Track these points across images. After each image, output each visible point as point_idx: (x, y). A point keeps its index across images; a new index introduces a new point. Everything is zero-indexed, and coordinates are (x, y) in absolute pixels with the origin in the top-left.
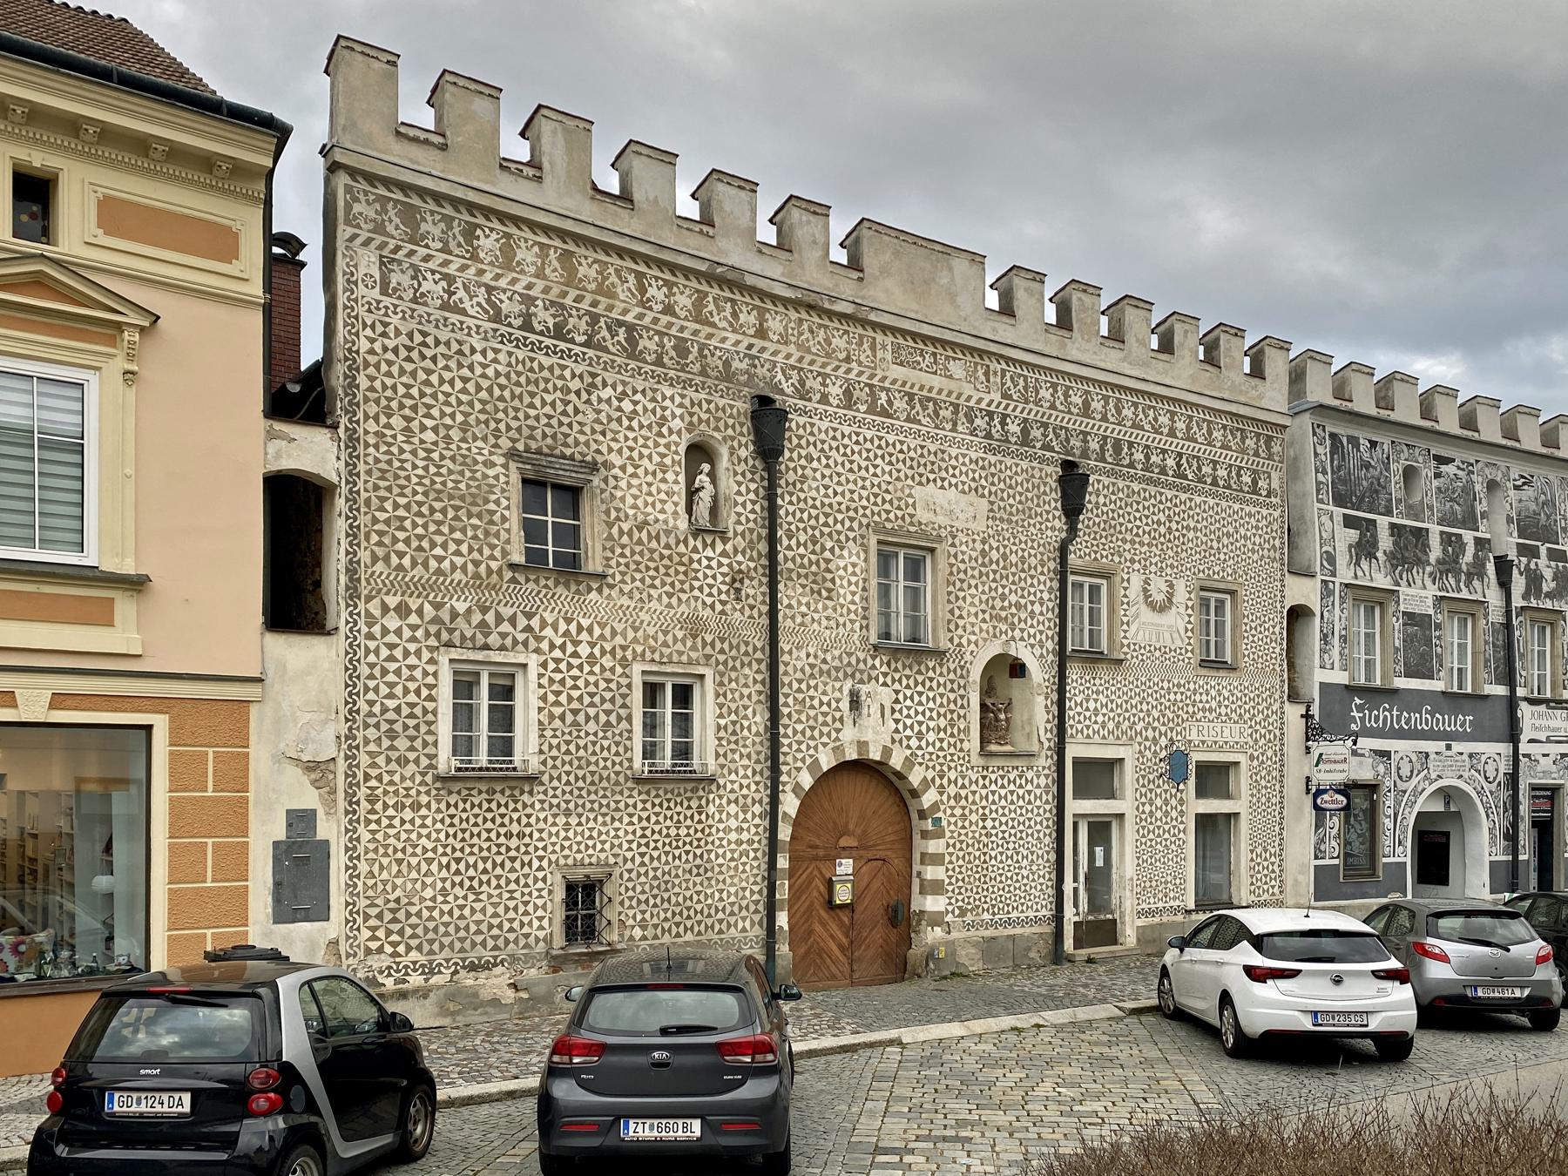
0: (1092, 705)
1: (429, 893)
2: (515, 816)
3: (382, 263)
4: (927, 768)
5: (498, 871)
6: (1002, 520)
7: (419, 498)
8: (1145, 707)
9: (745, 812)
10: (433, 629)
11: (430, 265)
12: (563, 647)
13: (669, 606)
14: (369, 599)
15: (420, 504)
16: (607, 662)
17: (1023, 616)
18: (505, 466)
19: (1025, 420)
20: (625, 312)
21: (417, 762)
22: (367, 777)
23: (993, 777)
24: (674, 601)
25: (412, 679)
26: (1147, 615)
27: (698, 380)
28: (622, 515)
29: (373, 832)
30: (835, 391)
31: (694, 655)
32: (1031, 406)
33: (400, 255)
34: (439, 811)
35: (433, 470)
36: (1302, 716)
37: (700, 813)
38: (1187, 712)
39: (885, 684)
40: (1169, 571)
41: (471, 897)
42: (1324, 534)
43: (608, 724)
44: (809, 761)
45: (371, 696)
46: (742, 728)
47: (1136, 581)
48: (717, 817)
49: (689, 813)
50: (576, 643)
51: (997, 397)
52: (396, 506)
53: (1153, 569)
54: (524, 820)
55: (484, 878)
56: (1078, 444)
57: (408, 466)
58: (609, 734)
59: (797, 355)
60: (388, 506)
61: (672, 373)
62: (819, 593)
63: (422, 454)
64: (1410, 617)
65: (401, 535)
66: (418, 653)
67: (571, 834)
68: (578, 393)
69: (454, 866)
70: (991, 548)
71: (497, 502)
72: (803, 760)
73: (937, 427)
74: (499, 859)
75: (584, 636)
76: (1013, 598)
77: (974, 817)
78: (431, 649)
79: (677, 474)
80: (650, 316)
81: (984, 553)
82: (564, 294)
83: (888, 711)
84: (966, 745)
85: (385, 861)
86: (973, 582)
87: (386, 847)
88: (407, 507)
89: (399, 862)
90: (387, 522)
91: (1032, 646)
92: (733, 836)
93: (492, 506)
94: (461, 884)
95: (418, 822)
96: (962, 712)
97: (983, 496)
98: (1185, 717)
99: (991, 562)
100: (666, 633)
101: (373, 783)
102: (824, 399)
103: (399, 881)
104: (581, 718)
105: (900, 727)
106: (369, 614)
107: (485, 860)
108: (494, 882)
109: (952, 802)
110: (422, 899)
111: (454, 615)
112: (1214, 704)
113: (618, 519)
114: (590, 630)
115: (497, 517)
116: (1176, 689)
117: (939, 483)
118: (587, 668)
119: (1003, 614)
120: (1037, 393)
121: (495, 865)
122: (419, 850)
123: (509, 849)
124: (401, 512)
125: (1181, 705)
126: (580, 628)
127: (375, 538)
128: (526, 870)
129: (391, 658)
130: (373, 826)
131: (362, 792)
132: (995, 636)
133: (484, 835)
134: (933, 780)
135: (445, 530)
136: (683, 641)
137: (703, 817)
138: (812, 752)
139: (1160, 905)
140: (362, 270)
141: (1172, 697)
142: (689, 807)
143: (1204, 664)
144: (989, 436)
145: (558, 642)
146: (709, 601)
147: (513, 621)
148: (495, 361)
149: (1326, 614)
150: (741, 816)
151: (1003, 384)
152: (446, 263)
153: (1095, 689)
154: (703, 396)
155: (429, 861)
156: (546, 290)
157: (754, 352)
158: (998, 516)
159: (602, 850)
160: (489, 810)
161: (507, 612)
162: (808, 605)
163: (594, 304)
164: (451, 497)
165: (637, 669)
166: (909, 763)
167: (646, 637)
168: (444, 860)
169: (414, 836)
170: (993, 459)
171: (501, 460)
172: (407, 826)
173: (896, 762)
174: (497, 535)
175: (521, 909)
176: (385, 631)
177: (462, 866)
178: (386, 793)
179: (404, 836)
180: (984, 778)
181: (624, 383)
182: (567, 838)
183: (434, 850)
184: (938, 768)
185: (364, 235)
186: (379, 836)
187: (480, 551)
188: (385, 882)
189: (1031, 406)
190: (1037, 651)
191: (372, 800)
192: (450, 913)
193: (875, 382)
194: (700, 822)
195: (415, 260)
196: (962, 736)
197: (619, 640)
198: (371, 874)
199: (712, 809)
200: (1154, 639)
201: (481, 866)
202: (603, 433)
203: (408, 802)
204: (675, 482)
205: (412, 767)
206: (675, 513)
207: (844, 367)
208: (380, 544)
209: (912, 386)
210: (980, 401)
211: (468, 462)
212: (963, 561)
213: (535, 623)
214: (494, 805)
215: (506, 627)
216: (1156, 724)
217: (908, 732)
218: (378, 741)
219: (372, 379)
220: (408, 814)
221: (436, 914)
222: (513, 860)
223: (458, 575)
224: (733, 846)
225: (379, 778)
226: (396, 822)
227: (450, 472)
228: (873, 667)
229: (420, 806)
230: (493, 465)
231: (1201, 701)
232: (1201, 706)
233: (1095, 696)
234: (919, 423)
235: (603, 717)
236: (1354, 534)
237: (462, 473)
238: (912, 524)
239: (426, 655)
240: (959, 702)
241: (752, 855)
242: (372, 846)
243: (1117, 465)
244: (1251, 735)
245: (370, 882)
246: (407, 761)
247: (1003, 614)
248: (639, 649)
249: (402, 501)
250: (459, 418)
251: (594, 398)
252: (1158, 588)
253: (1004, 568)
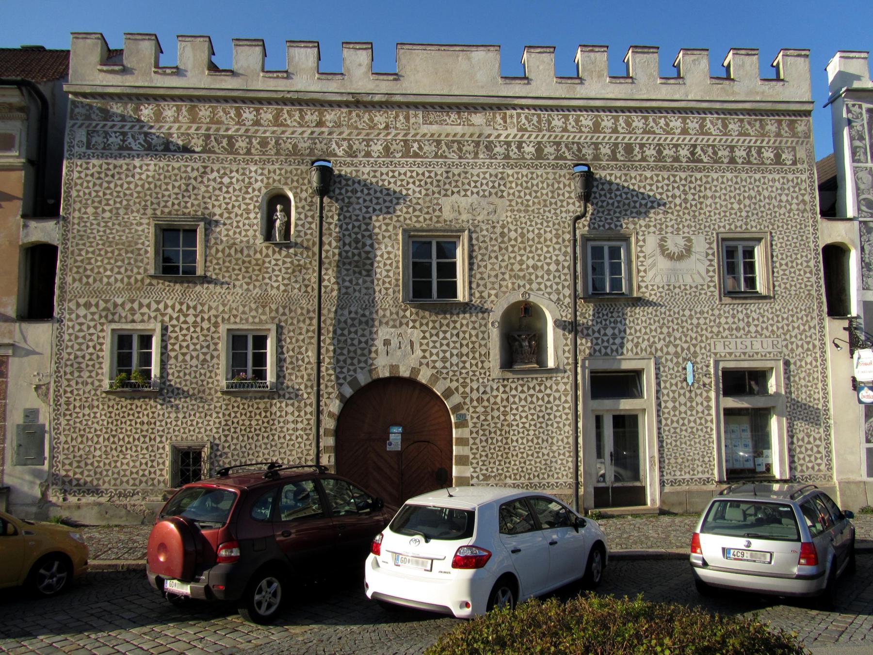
0: (609, 332)
1: (98, 453)
2: (146, 413)
3: (88, 134)
4: (451, 381)
5: (136, 443)
6: (519, 211)
7: (100, 247)
8: (665, 330)
9: (299, 411)
10: (104, 314)
11: (115, 129)
12: (178, 319)
13: (248, 290)
14: (70, 301)
15: (100, 250)
16: (205, 325)
17: (540, 274)
18: (148, 224)
19: (539, 143)
20: (227, 130)
21: (92, 383)
22: (65, 392)
23: (514, 386)
24: (251, 287)
25: (91, 340)
26: (663, 264)
27: (274, 158)
28: (219, 242)
29: (68, 420)
30: (377, 148)
31: (263, 318)
32: (544, 132)
33: (99, 128)
34: (103, 409)
35: (108, 231)
36: (845, 329)
37: (266, 412)
38: (711, 332)
39: (414, 327)
40: (686, 230)
41: (122, 456)
42: (862, 186)
43: (205, 360)
44: (349, 379)
45: (69, 350)
46: (297, 360)
47: (652, 242)
48: (278, 414)
49: (258, 412)
50: (186, 316)
51: (514, 131)
52: (87, 252)
53: (670, 230)
54: (151, 415)
55: (129, 446)
56: (590, 152)
57: (95, 231)
58: (206, 366)
59: (347, 132)
60: (83, 253)
61: (257, 158)
62: (360, 273)
63: (103, 224)
65: (89, 267)
66: (95, 327)
67: (179, 423)
68: (195, 179)
69: (112, 439)
70: (510, 230)
71: (143, 244)
72: (345, 378)
73: (460, 158)
74: (137, 436)
75: (191, 311)
76: (531, 262)
77: (496, 413)
78: (102, 324)
79: (257, 213)
80: (243, 129)
81: (502, 235)
82: (189, 128)
83: (417, 346)
84: (486, 365)
85: (74, 435)
86: (493, 255)
87: (74, 428)
88: (93, 252)
89: (82, 436)
90: (82, 261)
91: (549, 294)
92: (292, 426)
93: (140, 246)
94: (116, 449)
95: (92, 415)
96: (483, 342)
97: (502, 197)
98: (709, 335)
99: (510, 240)
100: (244, 306)
101: (69, 395)
102: (368, 154)
103: (82, 446)
104: (188, 358)
105: (427, 354)
106: (70, 309)
107: (129, 436)
108: (134, 449)
109: (475, 403)
110: (94, 457)
111: (116, 305)
112: (741, 325)
113: (216, 244)
114: (195, 308)
115: (142, 252)
116: (698, 315)
117: (463, 193)
118: (192, 329)
119: (521, 274)
120: (550, 123)
121: (134, 440)
122: (92, 430)
123: (142, 431)
124: (90, 255)
125: (704, 327)
126: (188, 307)
127: (75, 270)
128: (153, 442)
129: (81, 330)
130: (68, 417)
131: (63, 400)
132: (514, 289)
133: (128, 423)
134: (457, 389)
135: (112, 261)
136: (256, 310)
137: (268, 414)
138: (351, 373)
140: (77, 140)
141: (695, 321)
142: (258, 408)
143: (733, 294)
144: (507, 157)
145: (175, 315)
146: (275, 285)
147: (149, 306)
148: (148, 170)
150: (296, 414)
151: (518, 123)
152: (123, 127)
153: (612, 320)
154: (277, 166)
155: (98, 436)
156: (179, 128)
157: (315, 135)
158: (516, 208)
159: (199, 433)
160: (131, 409)
161: (145, 302)
162: (351, 281)
163: (208, 129)
164: (117, 244)
165: (223, 329)
166: (435, 378)
167: (231, 310)
168: (106, 436)
169: (90, 423)
171: (147, 221)
172: (87, 417)
173: (424, 377)
174: (142, 261)
175: (150, 464)
176: (78, 317)
177: (116, 439)
178: (75, 400)
179: (85, 422)
180: (505, 386)
181: (224, 168)
182: (176, 425)
183: (101, 430)
184: (461, 381)
185: (79, 122)
186: (71, 422)
187: (132, 271)
188: (74, 447)
189: (544, 132)
190: (554, 297)
191: (68, 403)
192: (110, 464)
193: (409, 137)
194: (266, 417)
195: (107, 129)
196: (483, 358)
197: (213, 312)
198: (66, 442)
199: (274, 409)
200: (673, 280)
201: (127, 439)
202: (210, 198)
203: (87, 404)
204: (256, 218)
205: (90, 387)
206: (255, 236)
207: (384, 133)
208: (78, 272)
209: (440, 135)
210: (499, 136)
211: (127, 225)
212: (484, 241)
213: (161, 306)
214: (134, 407)
215: (145, 310)
216: (678, 342)
217: (434, 358)
218: (72, 373)
219: (78, 191)
220: (87, 411)
221: (102, 464)
222: (145, 437)
223: (119, 284)
224: (291, 432)
225: (72, 392)
226: (81, 415)
227: (118, 231)
228: (404, 316)
229: (93, 407)
230: (141, 224)
231: (727, 323)
232: (726, 326)
233: (612, 325)
234: (446, 157)
235: (202, 357)
237: (124, 231)
238: (438, 222)
239: (99, 327)
240: (481, 336)
241: (305, 437)
242: (67, 427)
243: (630, 161)
244: (786, 346)
245: (66, 446)
246: (87, 384)
247: (521, 274)
248: (226, 316)
249: (91, 249)
250: (125, 203)
251: (205, 180)
252: (675, 243)
253: (522, 242)
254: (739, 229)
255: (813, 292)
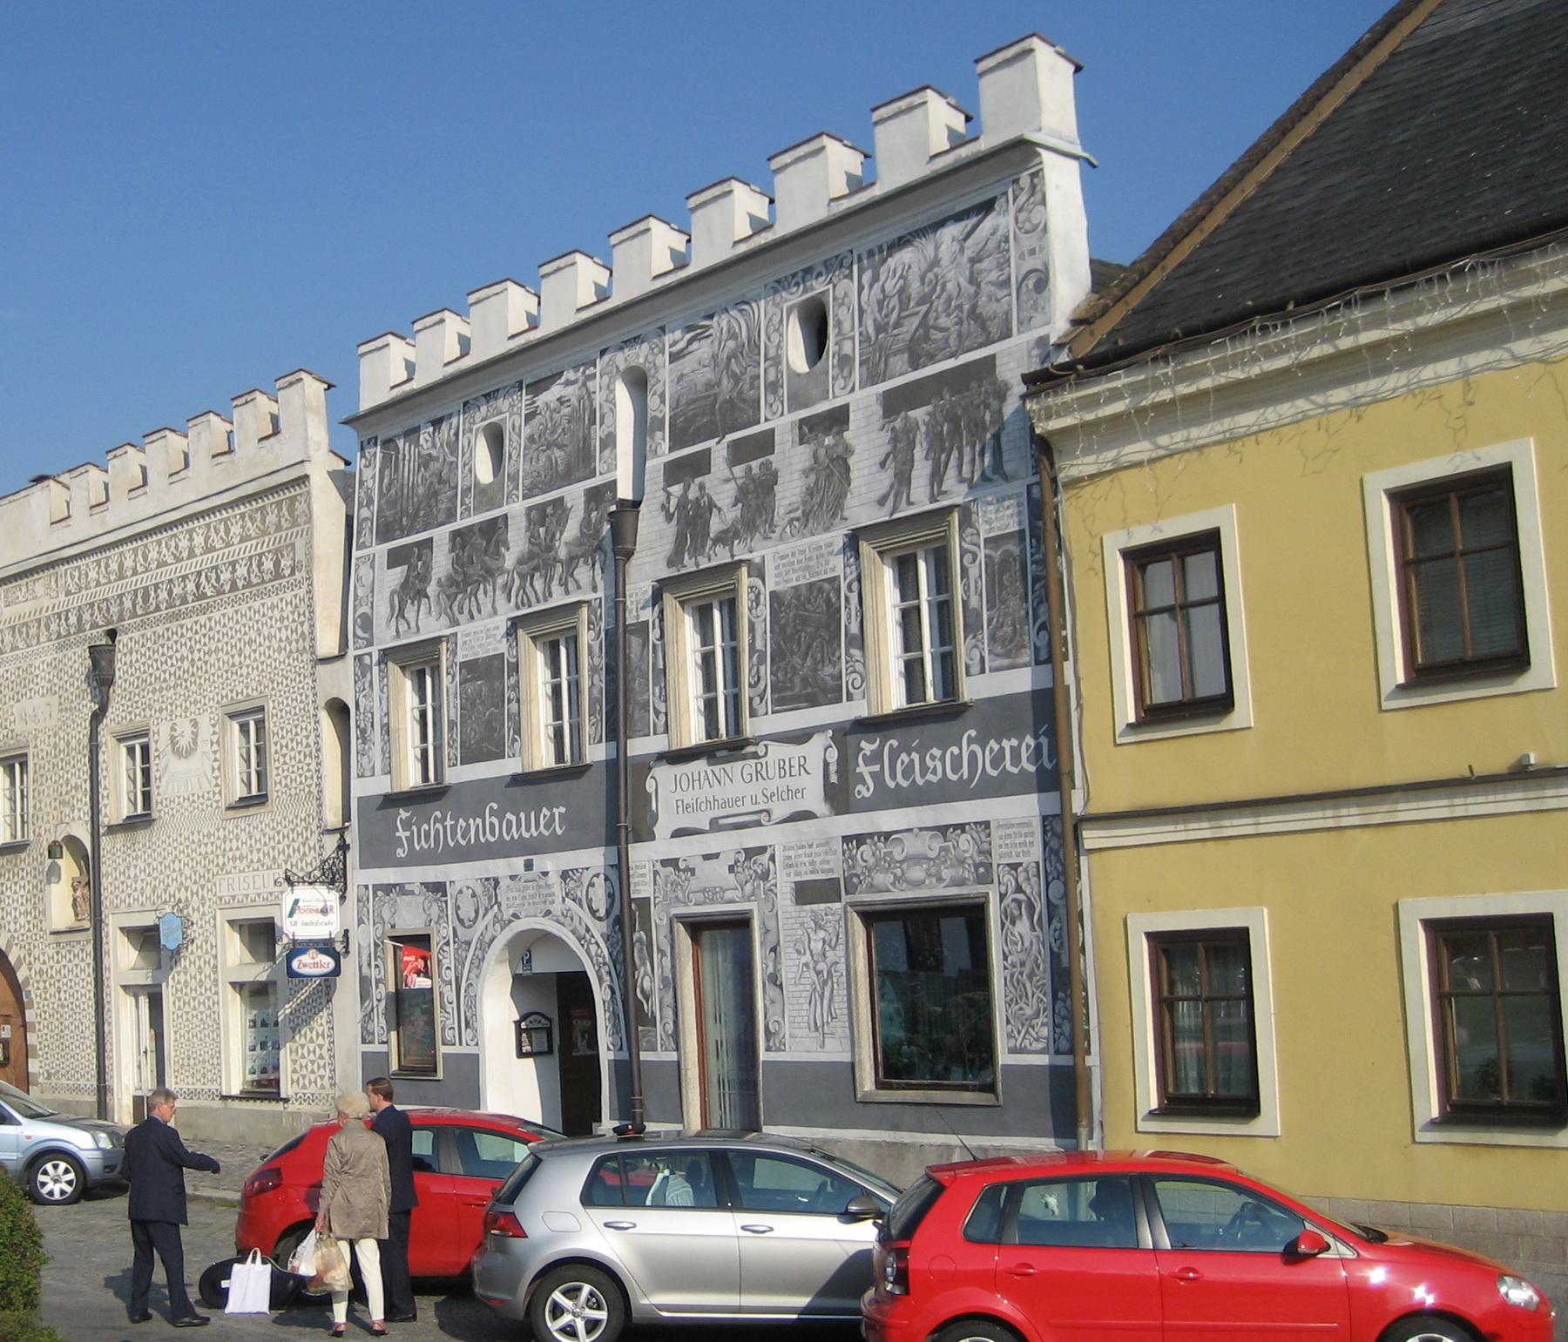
40: (193, 708)
42: (360, 593)
64: (472, 669)
112: (245, 850)
116: (206, 840)
139: (199, 1086)
149: (362, 702)
170: (60, 656)
196: (41, 917)
200: (182, 789)
231: (231, 850)
236: (399, 573)
243: (147, 614)
254: (240, 697)
255: (313, 789)
